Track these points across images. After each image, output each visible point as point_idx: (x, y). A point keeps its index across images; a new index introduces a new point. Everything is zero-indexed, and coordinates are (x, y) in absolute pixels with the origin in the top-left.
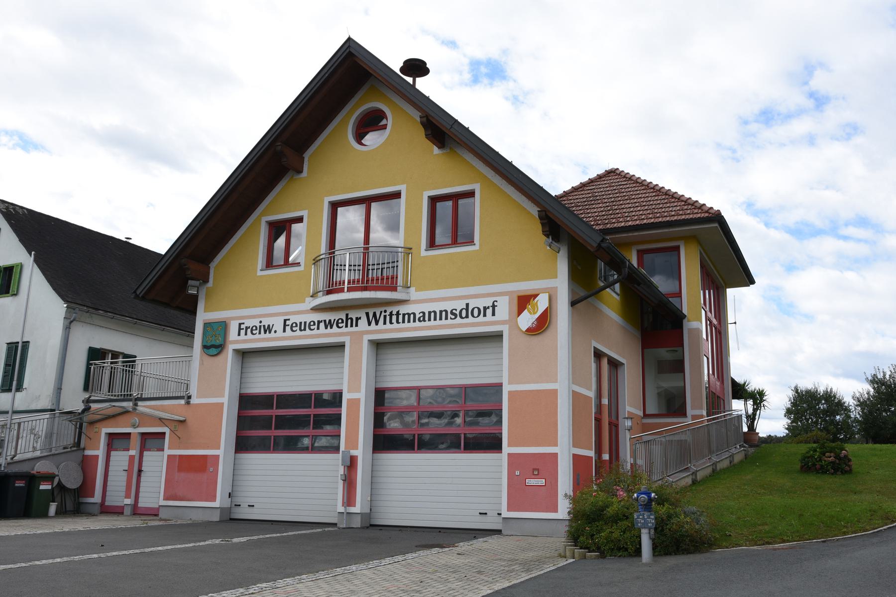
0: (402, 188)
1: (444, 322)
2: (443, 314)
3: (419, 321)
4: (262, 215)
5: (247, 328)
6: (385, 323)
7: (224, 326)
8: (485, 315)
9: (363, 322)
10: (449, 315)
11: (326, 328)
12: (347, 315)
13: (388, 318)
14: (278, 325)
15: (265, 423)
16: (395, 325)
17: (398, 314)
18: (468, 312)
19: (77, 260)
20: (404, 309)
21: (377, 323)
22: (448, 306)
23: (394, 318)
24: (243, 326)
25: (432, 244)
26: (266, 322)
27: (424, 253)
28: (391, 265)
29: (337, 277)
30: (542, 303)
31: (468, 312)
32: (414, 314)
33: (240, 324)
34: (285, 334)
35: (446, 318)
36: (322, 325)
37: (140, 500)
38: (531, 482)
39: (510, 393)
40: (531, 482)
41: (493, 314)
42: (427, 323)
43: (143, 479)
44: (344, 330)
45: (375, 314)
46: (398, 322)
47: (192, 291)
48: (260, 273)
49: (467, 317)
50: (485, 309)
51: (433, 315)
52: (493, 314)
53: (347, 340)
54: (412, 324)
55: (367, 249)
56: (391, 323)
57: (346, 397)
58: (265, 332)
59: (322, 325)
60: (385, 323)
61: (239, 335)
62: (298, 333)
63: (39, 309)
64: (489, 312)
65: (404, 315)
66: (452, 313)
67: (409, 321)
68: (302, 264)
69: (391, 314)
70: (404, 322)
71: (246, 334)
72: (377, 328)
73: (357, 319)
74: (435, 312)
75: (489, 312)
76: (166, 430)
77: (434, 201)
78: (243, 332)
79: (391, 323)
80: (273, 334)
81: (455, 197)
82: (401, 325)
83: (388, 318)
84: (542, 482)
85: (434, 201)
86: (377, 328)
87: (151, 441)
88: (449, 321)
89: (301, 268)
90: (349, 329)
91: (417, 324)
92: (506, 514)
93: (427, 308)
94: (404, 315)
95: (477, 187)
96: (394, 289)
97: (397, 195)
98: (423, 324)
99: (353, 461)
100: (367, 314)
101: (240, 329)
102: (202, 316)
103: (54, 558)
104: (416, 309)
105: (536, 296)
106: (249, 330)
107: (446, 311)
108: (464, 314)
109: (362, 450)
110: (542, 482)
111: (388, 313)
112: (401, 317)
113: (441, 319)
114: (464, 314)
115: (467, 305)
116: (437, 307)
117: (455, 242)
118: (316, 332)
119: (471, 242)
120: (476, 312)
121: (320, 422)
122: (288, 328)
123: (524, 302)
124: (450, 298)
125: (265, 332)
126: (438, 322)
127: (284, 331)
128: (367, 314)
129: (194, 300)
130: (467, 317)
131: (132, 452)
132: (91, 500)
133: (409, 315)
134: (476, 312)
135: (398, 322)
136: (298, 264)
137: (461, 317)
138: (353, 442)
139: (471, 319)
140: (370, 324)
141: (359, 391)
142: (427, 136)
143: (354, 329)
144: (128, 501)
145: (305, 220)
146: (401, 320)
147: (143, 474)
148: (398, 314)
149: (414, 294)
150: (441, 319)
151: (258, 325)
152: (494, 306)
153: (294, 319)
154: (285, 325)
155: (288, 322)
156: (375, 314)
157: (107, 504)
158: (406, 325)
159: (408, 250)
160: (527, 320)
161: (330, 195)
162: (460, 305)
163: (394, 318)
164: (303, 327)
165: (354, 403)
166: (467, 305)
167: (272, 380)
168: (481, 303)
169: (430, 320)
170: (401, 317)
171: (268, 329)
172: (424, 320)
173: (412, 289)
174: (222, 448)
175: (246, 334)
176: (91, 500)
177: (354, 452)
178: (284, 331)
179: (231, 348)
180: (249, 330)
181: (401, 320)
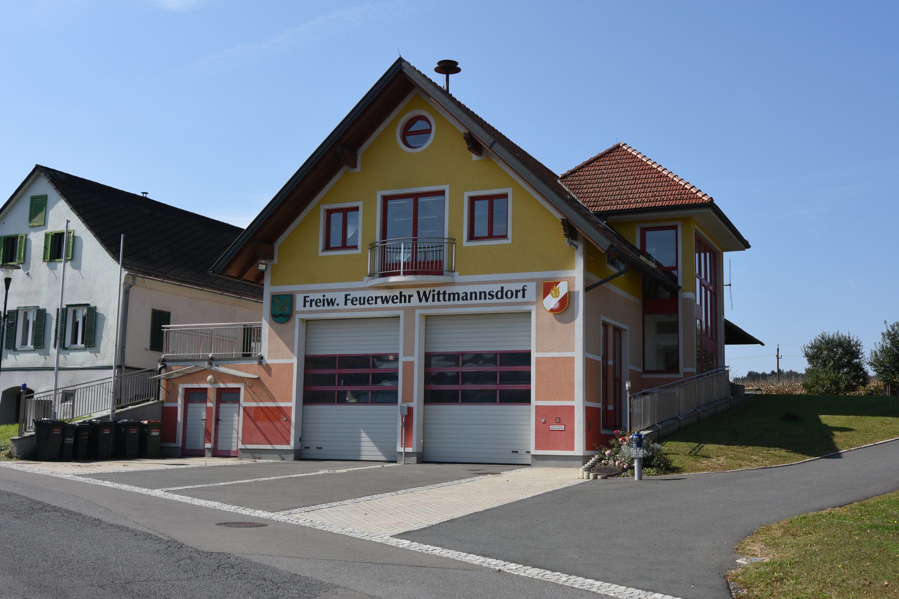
0: (446, 188)
1: (483, 301)
2: (482, 295)
3: (463, 299)
4: (323, 202)
5: (312, 301)
6: (433, 301)
7: (290, 298)
8: (516, 297)
9: (415, 299)
10: (488, 296)
11: (383, 303)
12: (401, 293)
13: (436, 296)
14: (340, 298)
15: (330, 380)
16: (442, 303)
17: (444, 293)
18: (502, 293)
19: (151, 236)
20: (449, 290)
21: (427, 300)
22: (487, 288)
23: (441, 297)
24: (307, 299)
25: (472, 237)
26: (329, 296)
27: (466, 244)
28: (434, 249)
29: (391, 258)
30: (563, 289)
31: (502, 293)
32: (458, 294)
33: (305, 297)
34: (346, 307)
35: (485, 298)
36: (379, 300)
37: (219, 444)
38: (553, 427)
39: (537, 358)
40: (553, 427)
41: (524, 296)
42: (469, 302)
43: (220, 427)
44: (398, 305)
45: (425, 292)
46: (444, 300)
47: (262, 267)
48: (321, 254)
49: (502, 297)
50: (517, 292)
51: (474, 295)
52: (524, 296)
53: (401, 313)
54: (456, 302)
55: (416, 240)
56: (439, 300)
57: (402, 359)
58: (329, 305)
59: (379, 300)
60: (433, 301)
61: (305, 306)
62: (358, 306)
63: (99, 276)
64: (520, 294)
65: (450, 294)
66: (489, 294)
67: (454, 300)
68: (360, 246)
69: (439, 293)
70: (449, 300)
71: (311, 306)
72: (427, 304)
73: (410, 296)
74: (476, 293)
75: (520, 294)
76: (241, 386)
77: (473, 200)
78: (308, 304)
79: (439, 300)
80: (335, 307)
81: (491, 198)
82: (447, 303)
83: (436, 296)
84: (562, 427)
85: (473, 200)
86: (427, 304)
87: (227, 396)
88: (487, 301)
89: (359, 251)
90: (403, 304)
91: (461, 302)
92: (534, 452)
93: (469, 289)
94: (450, 294)
95: (509, 191)
96: (441, 274)
97: (442, 193)
98: (465, 302)
99: (410, 410)
100: (418, 293)
101: (305, 301)
102: (269, 289)
103: (194, 484)
104: (461, 290)
105: (558, 283)
106: (314, 303)
107: (485, 293)
108: (499, 295)
109: (417, 403)
110: (562, 427)
111: (436, 293)
112: (447, 296)
113: (480, 299)
114: (499, 295)
115: (502, 288)
116: (478, 289)
117: (491, 236)
118: (374, 306)
119: (505, 237)
120: (509, 294)
121: (379, 378)
122: (349, 302)
123: (548, 288)
124: (488, 282)
125: (329, 305)
126: (478, 301)
127: (346, 304)
128: (418, 293)
129: (261, 275)
130: (502, 297)
131: (210, 405)
132: (173, 445)
133: (454, 294)
134: (509, 294)
135: (444, 300)
136: (355, 247)
137: (497, 298)
138: (408, 398)
139: (505, 300)
140: (420, 300)
141: (412, 355)
142: (469, 149)
143: (407, 304)
144: (208, 445)
145: (361, 209)
146: (447, 298)
147: (220, 423)
148: (444, 293)
149: (457, 277)
150: (480, 299)
151: (322, 298)
152: (524, 290)
153: (353, 294)
154: (346, 300)
155: (348, 297)
156: (425, 292)
157: (187, 448)
158: (452, 302)
159: (452, 241)
160: (551, 302)
161: (383, 190)
162: (496, 288)
163: (441, 297)
164: (362, 301)
165: (409, 366)
166: (502, 288)
167: (335, 344)
168: (514, 287)
169: (471, 299)
170: (447, 296)
171: (331, 302)
172: (467, 299)
173: (457, 274)
174: (291, 403)
175: (311, 306)
176: (173, 445)
177: (411, 405)
178: (346, 304)
179: (298, 317)
180: (314, 303)
181: (447, 298)
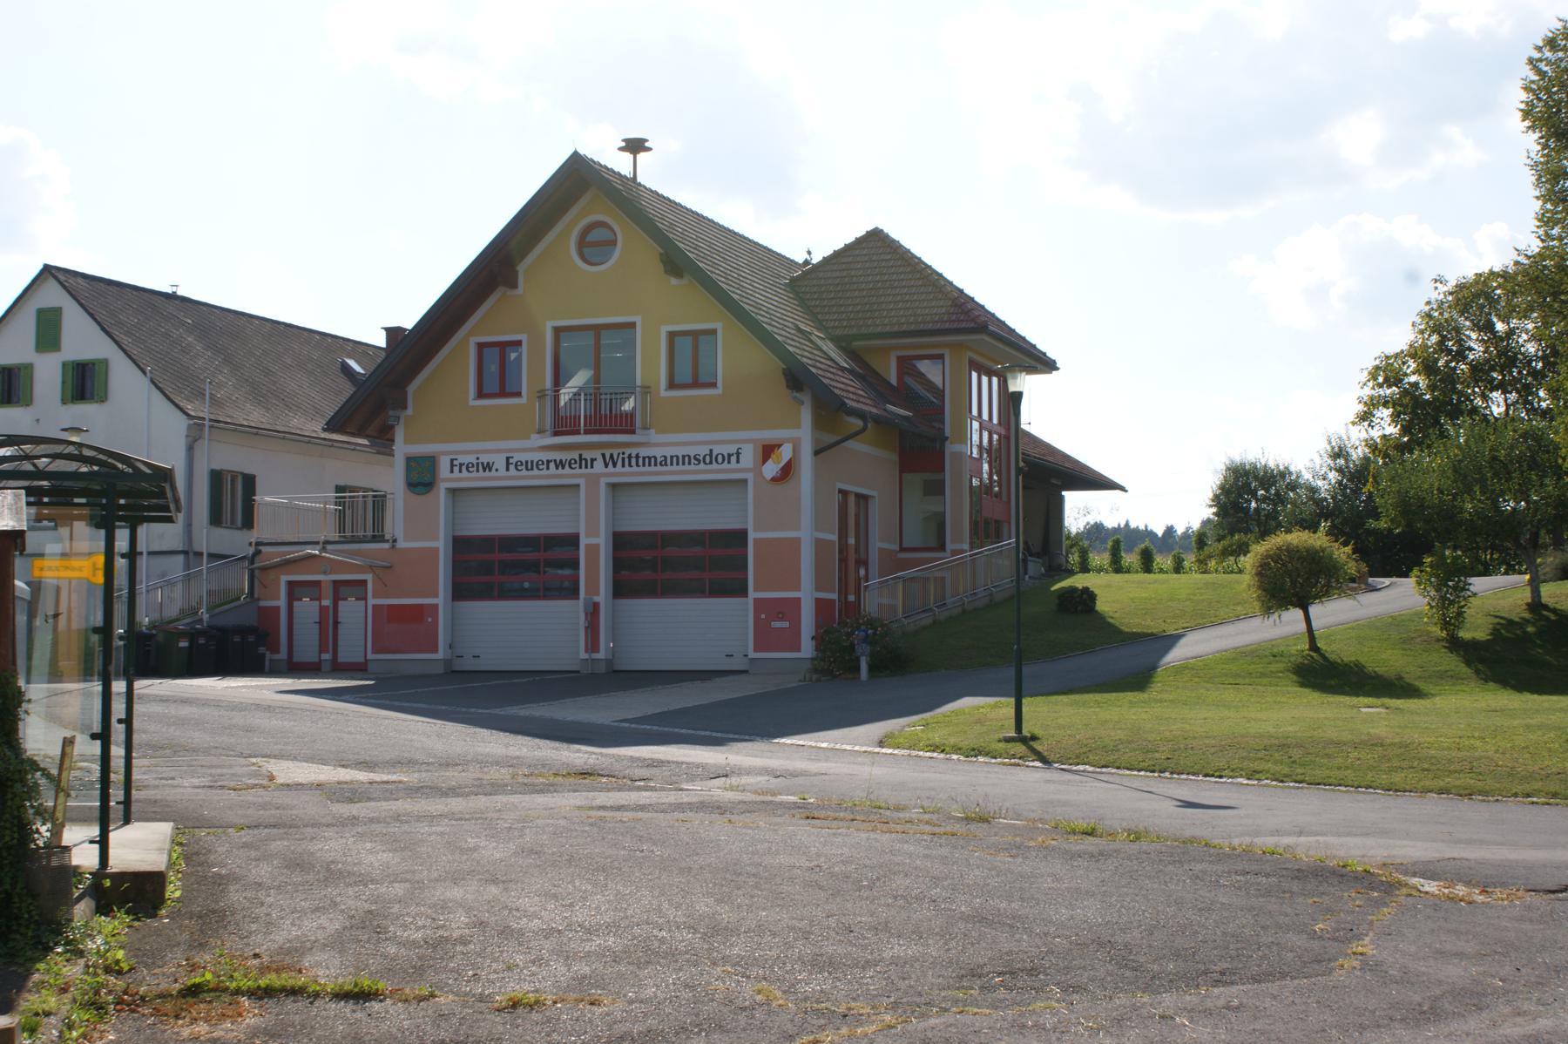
1: (687, 467)
2: (686, 459)
7: (431, 462)
9: (599, 464)
14: (500, 462)
16: (635, 469)
18: (711, 458)
20: (644, 452)
21: (615, 465)
22: (692, 451)
26: (485, 459)
30: (786, 453)
36: (552, 465)
42: (669, 468)
44: (578, 471)
48: (473, 403)
51: (675, 460)
54: (653, 468)
59: (552, 465)
62: (524, 472)
64: (734, 459)
73: (593, 460)
75: (734, 459)
76: (369, 577)
77: (672, 336)
78: (456, 469)
81: (695, 334)
82: (642, 469)
84: (786, 624)
85: (672, 336)
88: (692, 467)
89: (523, 400)
90: (583, 470)
91: (659, 468)
92: (752, 655)
93: (669, 451)
96: (633, 432)
105: (779, 446)
109: (603, 596)
110: (786, 624)
116: (680, 451)
118: (545, 472)
122: (512, 467)
123: (768, 451)
124: (692, 442)
126: (681, 467)
138: (593, 588)
139: (715, 466)
143: (589, 470)
152: (738, 454)
153: (517, 457)
158: (647, 469)
160: (771, 469)
162: (703, 451)
164: (530, 466)
165: (593, 550)
171: (488, 467)
174: (441, 599)
177: (596, 599)
179: (442, 487)
